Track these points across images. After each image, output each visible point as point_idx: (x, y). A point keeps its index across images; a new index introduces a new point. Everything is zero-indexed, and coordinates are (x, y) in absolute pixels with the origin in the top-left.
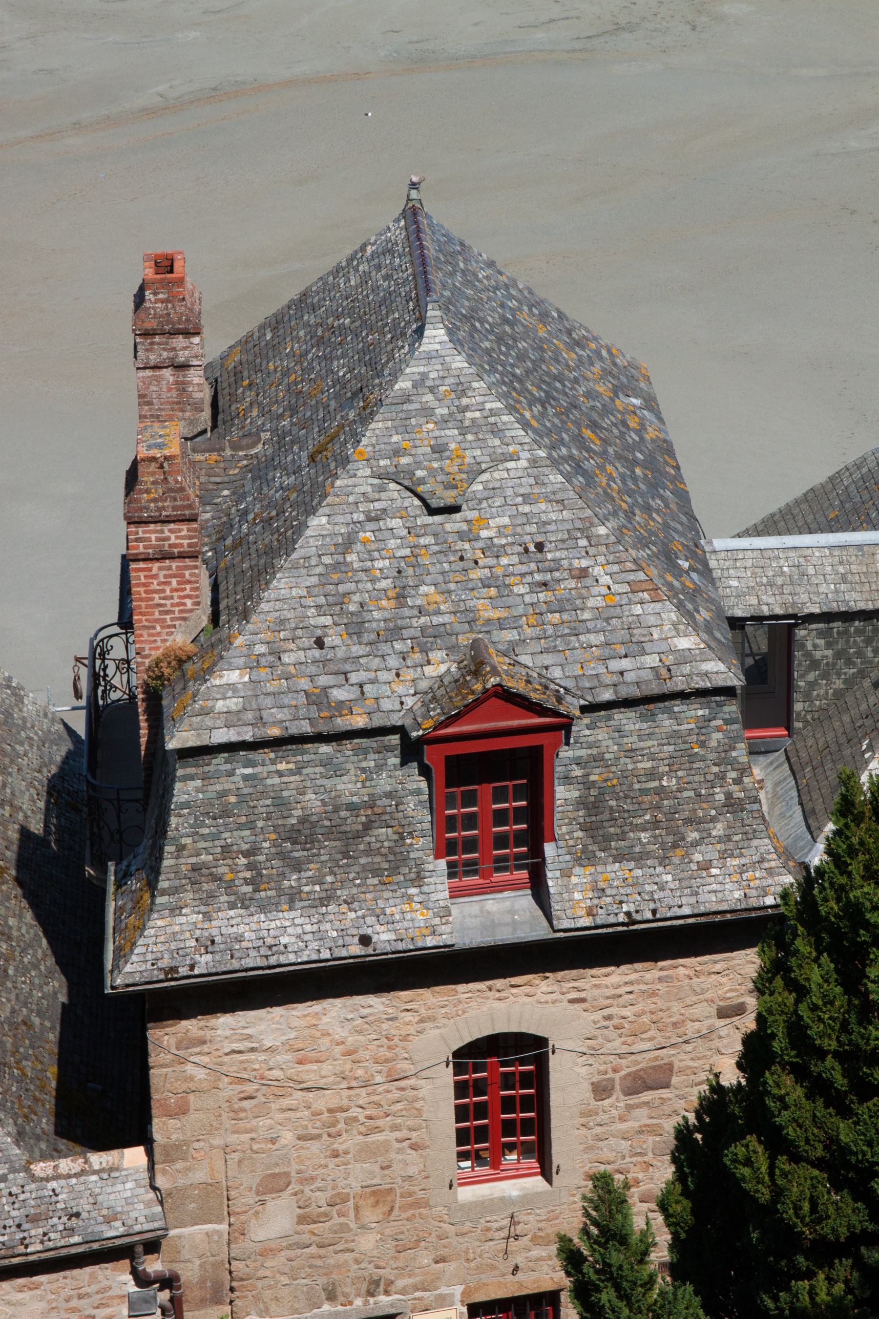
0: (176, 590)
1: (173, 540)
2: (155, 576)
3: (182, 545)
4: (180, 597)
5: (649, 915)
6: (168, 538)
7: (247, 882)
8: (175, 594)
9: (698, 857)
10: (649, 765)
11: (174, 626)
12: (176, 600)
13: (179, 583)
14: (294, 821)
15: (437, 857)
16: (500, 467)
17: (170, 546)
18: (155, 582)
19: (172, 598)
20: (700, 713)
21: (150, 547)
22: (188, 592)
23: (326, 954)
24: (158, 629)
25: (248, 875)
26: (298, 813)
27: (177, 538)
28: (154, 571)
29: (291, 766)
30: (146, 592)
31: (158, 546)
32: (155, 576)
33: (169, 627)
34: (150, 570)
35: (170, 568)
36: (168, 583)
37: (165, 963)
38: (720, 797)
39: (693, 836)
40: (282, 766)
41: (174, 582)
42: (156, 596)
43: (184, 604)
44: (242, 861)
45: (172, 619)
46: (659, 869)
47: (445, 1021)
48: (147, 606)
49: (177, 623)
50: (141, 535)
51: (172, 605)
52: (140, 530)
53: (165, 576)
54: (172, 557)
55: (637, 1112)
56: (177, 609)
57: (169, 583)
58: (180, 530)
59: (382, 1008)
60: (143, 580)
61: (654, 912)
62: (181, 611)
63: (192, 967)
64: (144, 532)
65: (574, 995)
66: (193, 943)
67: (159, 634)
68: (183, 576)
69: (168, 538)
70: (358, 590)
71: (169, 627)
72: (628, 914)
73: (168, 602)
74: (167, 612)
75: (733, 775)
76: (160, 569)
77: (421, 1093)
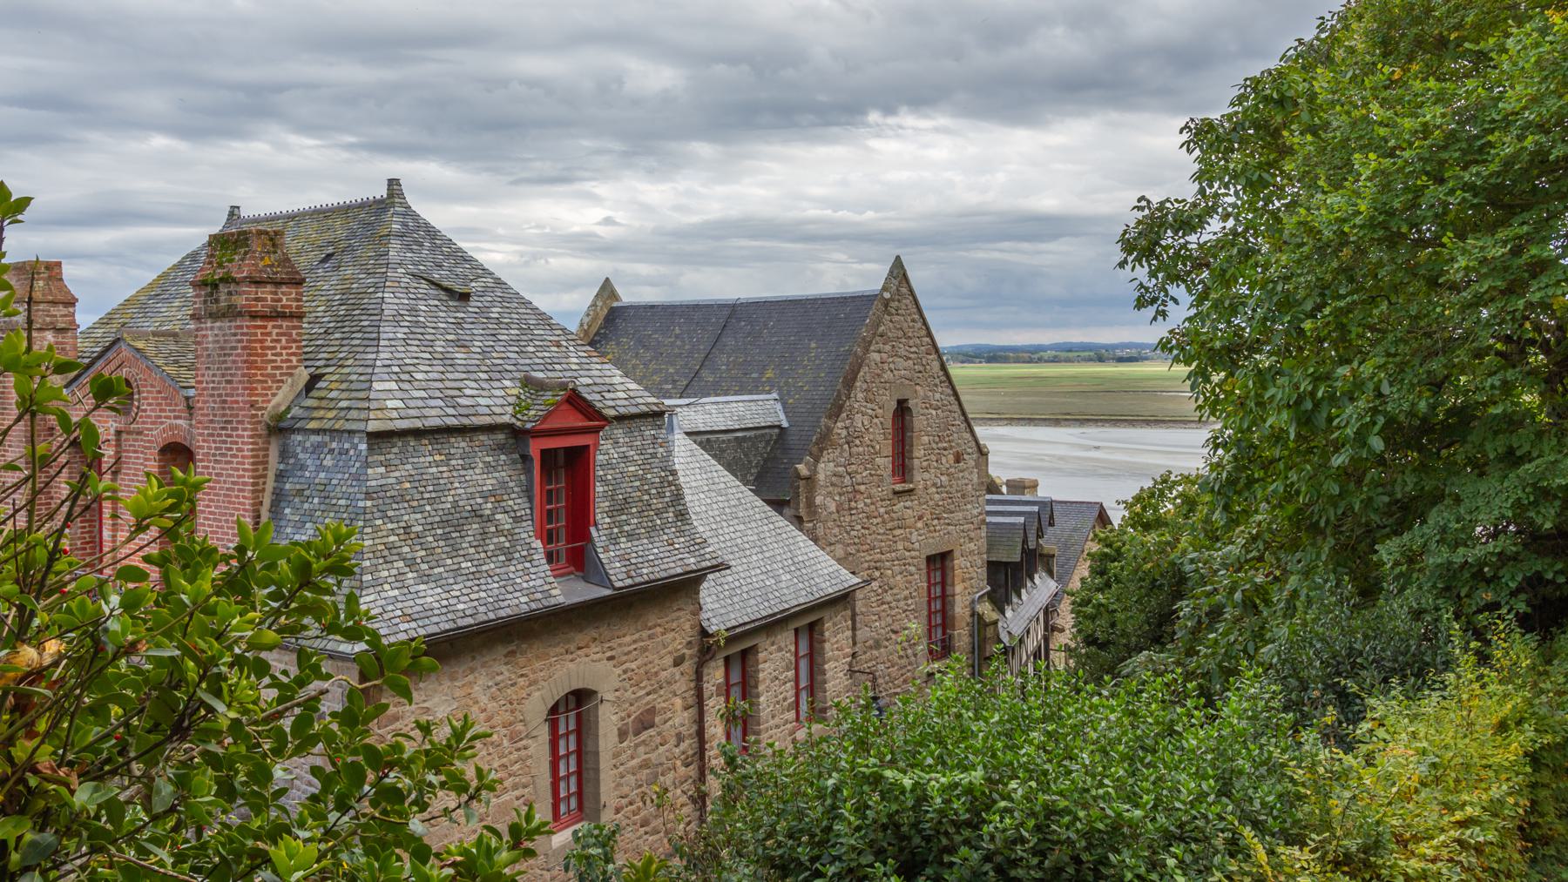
0: (285, 348)
1: (284, 302)
2: (269, 334)
3: (291, 306)
4: (288, 354)
11: (282, 381)
12: (285, 357)
13: (287, 341)
17: (282, 306)
19: (281, 354)
21: (267, 306)
22: (293, 350)
23: (492, 616)
30: (262, 348)
31: (272, 306)
32: (269, 334)
33: (279, 381)
34: (265, 327)
35: (280, 327)
36: (278, 341)
40: (437, 458)
41: (284, 339)
43: (291, 361)
45: (281, 374)
47: (543, 683)
48: (262, 361)
51: (282, 361)
53: (277, 334)
54: (283, 316)
55: (641, 749)
58: (291, 294)
59: (507, 674)
60: (259, 337)
62: (288, 368)
64: (263, 293)
65: (609, 654)
67: (270, 388)
68: (291, 335)
69: (280, 300)
71: (279, 381)
74: (280, 368)
76: (274, 327)
77: (531, 751)
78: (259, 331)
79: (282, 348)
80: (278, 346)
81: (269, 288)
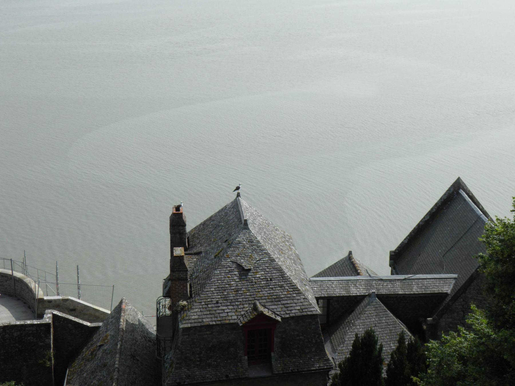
1: (182, 276)
5: (296, 370)
6: (181, 276)
7: (198, 361)
8: (182, 289)
9: (308, 356)
10: (297, 333)
12: (182, 291)
13: (183, 287)
14: (210, 346)
15: (245, 355)
16: (262, 260)
18: (177, 286)
19: (181, 290)
20: (310, 320)
24: (177, 297)
25: (199, 359)
26: (211, 344)
27: (183, 276)
28: (177, 283)
29: (210, 332)
37: (178, 381)
38: (314, 341)
39: (307, 351)
40: (208, 333)
41: (182, 286)
42: (177, 290)
43: (184, 292)
44: (198, 356)
46: (299, 359)
49: (182, 296)
50: (174, 275)
51: (181, 292)
52: (174, 273)
53: (180, 285)
56: (182, 293)
57: (180, 287)
58: (184, 274)
61: (298, 370)
63: (184, 382)
66: (185, 376)
69: (181, 276)
70: (227, 289)
72: (291, 370)
73: (180, 291)
74: (180, 294)
75: (317, 336)
76: (178, 283)
78: (174, 284)
79: (181, 288)
80: (180, 288)
81: (177, 273)
